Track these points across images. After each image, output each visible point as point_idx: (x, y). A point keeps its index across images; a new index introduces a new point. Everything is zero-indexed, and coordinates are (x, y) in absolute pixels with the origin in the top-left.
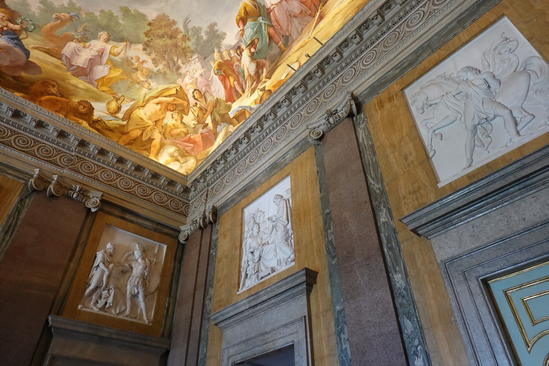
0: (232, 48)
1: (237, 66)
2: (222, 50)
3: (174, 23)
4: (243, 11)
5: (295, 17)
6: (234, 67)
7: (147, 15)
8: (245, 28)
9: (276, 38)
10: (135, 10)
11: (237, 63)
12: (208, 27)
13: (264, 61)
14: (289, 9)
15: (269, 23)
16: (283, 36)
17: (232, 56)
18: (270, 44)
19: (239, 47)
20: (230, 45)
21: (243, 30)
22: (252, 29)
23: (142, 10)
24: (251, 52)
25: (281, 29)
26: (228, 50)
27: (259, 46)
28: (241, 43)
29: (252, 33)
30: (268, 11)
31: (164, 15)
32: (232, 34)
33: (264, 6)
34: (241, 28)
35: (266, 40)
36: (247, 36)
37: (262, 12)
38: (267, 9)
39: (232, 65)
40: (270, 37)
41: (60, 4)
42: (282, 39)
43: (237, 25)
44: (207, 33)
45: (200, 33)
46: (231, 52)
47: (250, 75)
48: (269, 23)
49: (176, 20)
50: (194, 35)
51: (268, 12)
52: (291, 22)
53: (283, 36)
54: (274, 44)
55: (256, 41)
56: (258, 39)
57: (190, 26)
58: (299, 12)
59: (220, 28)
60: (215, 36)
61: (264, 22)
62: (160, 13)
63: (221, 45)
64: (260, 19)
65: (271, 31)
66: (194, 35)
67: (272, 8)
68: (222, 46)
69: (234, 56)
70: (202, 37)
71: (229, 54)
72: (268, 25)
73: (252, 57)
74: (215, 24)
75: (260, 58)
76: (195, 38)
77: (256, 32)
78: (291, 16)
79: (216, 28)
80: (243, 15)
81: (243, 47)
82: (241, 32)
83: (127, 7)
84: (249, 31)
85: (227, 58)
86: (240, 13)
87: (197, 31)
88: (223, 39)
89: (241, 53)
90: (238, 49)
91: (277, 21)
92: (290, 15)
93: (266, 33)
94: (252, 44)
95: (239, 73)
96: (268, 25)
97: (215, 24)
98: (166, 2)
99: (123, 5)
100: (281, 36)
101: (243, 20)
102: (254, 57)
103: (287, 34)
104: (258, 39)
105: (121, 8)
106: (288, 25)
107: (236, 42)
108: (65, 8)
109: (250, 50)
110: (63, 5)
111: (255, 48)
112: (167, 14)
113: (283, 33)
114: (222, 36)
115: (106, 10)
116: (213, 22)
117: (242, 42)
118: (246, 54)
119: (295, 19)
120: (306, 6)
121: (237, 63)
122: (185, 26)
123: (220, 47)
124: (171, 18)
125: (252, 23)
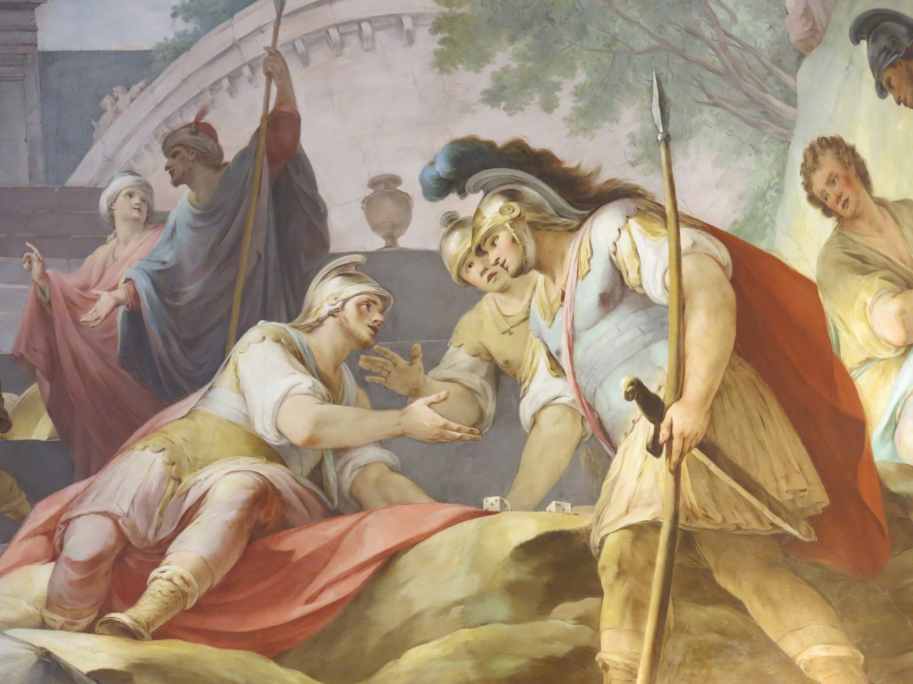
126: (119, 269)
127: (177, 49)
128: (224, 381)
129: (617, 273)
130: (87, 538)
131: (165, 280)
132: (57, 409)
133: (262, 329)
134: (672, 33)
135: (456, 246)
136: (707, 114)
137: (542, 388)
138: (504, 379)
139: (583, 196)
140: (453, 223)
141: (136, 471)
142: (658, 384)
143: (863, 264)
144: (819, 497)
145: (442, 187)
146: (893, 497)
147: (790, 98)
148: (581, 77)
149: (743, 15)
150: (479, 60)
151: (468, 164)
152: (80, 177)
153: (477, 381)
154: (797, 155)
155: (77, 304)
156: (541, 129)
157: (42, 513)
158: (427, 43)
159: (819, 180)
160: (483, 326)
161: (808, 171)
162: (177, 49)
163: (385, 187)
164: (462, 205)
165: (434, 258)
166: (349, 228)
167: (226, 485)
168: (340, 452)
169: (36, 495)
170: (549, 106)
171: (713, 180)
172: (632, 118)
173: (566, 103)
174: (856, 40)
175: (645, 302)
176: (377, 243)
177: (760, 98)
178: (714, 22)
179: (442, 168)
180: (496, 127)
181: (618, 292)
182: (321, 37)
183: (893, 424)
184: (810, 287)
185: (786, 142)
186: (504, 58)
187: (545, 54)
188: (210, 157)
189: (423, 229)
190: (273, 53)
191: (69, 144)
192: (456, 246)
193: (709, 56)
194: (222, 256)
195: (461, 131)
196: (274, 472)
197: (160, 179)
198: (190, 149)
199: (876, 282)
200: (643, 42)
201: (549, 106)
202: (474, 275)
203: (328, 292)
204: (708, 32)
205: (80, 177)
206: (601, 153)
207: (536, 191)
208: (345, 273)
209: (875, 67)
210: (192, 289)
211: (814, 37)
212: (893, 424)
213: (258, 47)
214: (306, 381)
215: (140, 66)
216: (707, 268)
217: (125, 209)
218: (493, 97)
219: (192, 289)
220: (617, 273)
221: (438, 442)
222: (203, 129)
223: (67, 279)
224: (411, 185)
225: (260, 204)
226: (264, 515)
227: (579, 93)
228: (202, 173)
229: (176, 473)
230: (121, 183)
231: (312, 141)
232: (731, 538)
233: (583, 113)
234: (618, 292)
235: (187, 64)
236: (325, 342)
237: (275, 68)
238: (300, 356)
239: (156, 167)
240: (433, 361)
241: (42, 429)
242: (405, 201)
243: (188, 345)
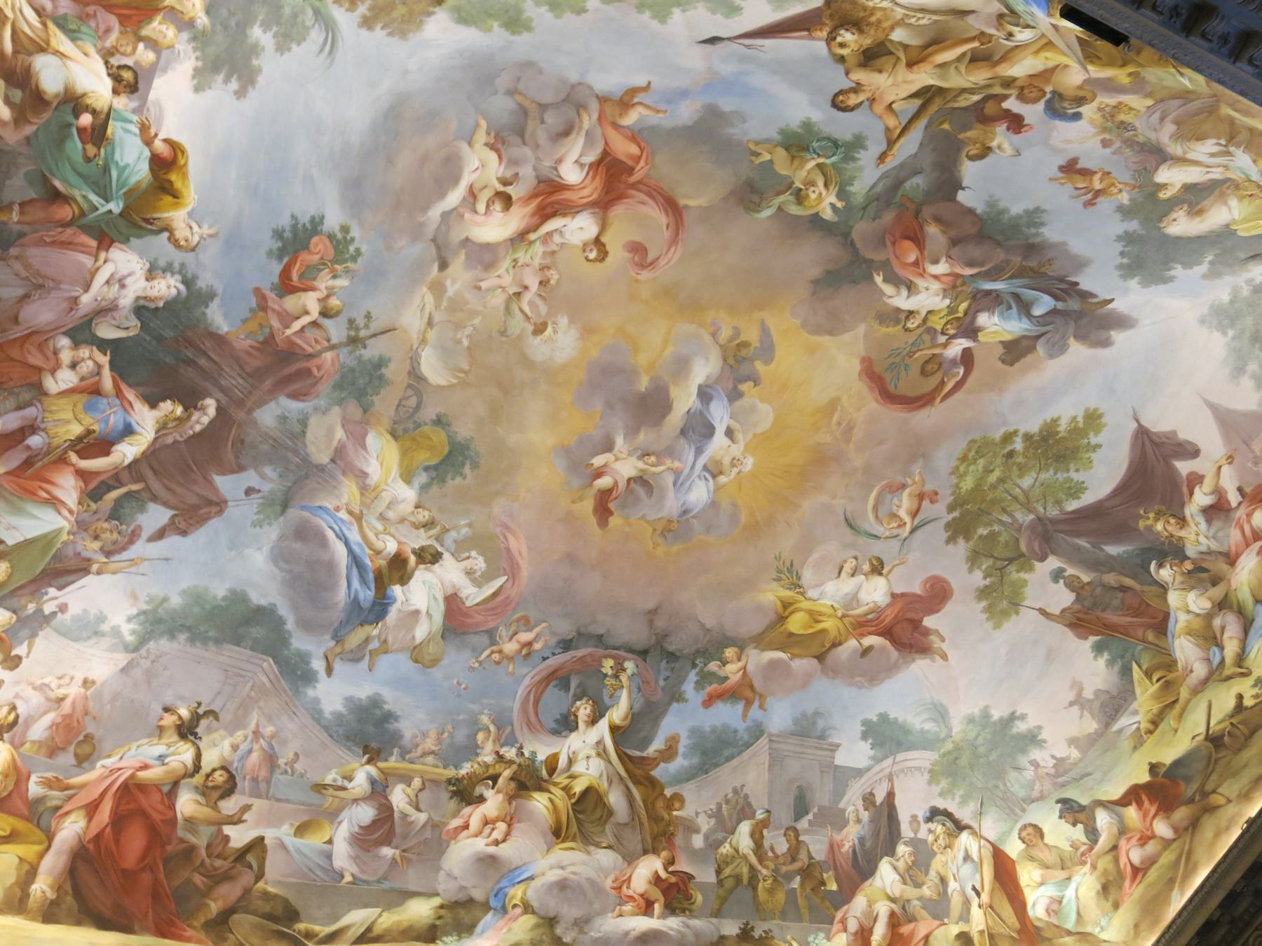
0: (152, 70)
1: (108, 31)
2: (185, 36)
3: (367, 23)
4: (178, 184)
5: (25, 297)
6: (113, 21)
7: (452, 25)
8: (147, 153)
9: (38, 213)
10: (490, 30)
11: (111, 41)
12: (259, 70)
13: (29, 130)
14: (54, 294)
15: (84, 221)
16: (21, 235)
17: (141, 46)
18: (45, 181)
19: (132, 88)
20: (165, 70)
21: (148, 143)
22: (127, 166)
23: (470, 37)
24: (87, 109)
25: (41, 243)
26: (165, 54)
27: (75, 146)
28: (134, 104)
29: (117, 157)
30: (107, 240)
31: (403, 35)
32: (180, 102)
33: (126, 240)
34: (159, 145)
35: (65, 181)
36: (127, 137)
37: (122, 225)
38: (112, 242)
39: (123, 20)
40: (56, 197)
41: (691, 13)
42: (19, 227)
43: (175, 137)
44: (255, 49)
45: (275, 36)
46: (150, 56)
47: (42, 48)
48: (84, 221)
49: (364, 32)
50: (295, 16)
51: (105, 236)
52: (26, 279)
53: (21, 235)
54: (32, 194)
55: (91, 150)
56: (88, 160)
57: (316, 35)
58: (23, 315)
59: (221, 91)
60: (228, 61)
61: (102, 210)
62: (414, 38)
63: (195, 49)
64: (116, 207)
65: (66, 212)
66: (295, 16)
67: (103, 255)
68: (190, 47)
69: (135, 49)
70: (266, 26)
71: (153, 44)
72: (83, 214)
73: (73, 102)
74: (240, 94)
75: (46, 125)
76: (287, 11)
77: (106, 169)
78: (38, 285)
79: (234, 85)
80: (173, 177)
81: (123, 103)
82: (153, 132)
83: (513, 33)
84: (131, 158)
85: (158, 28)
86: (184, 176)
87: (288, 37)
88: (197, 72)
89: (116, 79)
90: (129, 82)
91: (68, 245)
92: (41, 286)
93: (77, 194)
94: (98, 134)
95: (84, 18)
96: (83, 214)
97: (240, 94)
98: (406, 72)
99: (526, 37)
100: (26, 228)
101: (166, 165)
102: (68, 108)
103: (13, 251)
104: (88, 160)
105: (529, 28)
106: (27, 266)
107: (152, 96)
108: (679, 5)
109: (94, 112)
110: (684, 11)
111: (81, 131)
112: (395, 41)
113: (26, 240)
114: (201, 79)
115: (569, 16)
116: (252, 94)
117: (134, 111)
118: (94, 82)
119: (20, 292)
120: (15, 340)
121: (111, 41)
122: (330, 27)
123: (194, 39)
124: (379, 33)
125: (133, 180)
126: (850, 836)
127: (868, 769)
128: (878, 874)
129: (966, 851)
130: (853, 926)
131: (862, 840)
132: (838, 880)
133: (886, 860)
134: (990, 785)
135: (931, 838)
136: (994, 808)
137: (953, 885)
138: (943, 880)
139: (960, 827)
140: (930, 831)
141: (859, 903)
142: (978, 887)
143: (1032, 859)
144: (1017, 925)
145: (929, 820)
146: (1036, 927)
147: (1024, 811)
148: (962, 792)
149: (1016, 787)
150: (938, 783)
151: (934, 814)
152: (841, 805)
153: (937, 881)
154: (1019, 825)
155: (840, 846)
156: (952, 807)
157: (839, 915)
158: (927, 776)
159: (1024, 834)
160: (937, 864)
161: (1021, 831)
162: (868, 769)
163: (914, 817)
164: (932, 826)
165: (925, 841)
166: (906, 830)
167: (883, 909)
168: (908, 901)
169: (837, 908)
170: (953, 799)
171: (991, 827)
172: (973, 806)
173: (957, 799)
174: (1058, 802)
175: (973, 861)
176: (912, 835)
177: (1012, 806)
178: (1005, 785)
179: (928, 814)
180: (941, 804)
181: (967, 857)
182: (902, 770)
183: (1034, 905)
184: (1013, 862)
185: (1016, 821)
186: (944, 783)
187: (954, 784)
188: (873, 803)
189: (922, 834)
190: (891, 774)
191: (839, 794)
192: (931, 838)
193: (1000, 795)
194: (876, 834)
195: (933, 804)
196: (893, 905)
197: (861, 808)
198: (868, 799)
199: (1035, 864)
200: (980, 786)
201: (953, 799)
202: (935, 848)
203: (902, 849)
204: (1002, 787)
205: (841, 805)
206: (964, 814)
207: (949, 824)
208: (905, 844)
209: (1061, 811)
210: (868, 844)
211: (1041, 798)
212: (1034, 905)
213: (887, 772)
214: (898, 877)
215: (859, 773)
216: (987, 852)
217: (852, 817)
218: (941, 794)
219: (868, 844)
220: (966, 851)
221: (930, 900)
222: (872, 794)
223: (837, 837)
224: (921, 819)
225: (885, 819)
226: (894, 922)
227: (961, 796)
228: (871, 808)
229: (870, 904)
230: (851, 808)
231: (898, 802)
232: (1001, 935)
233: (961, 803)
234: (967, 857)
235: (869, 774)
236: (901, 865)
237: (891, 779)
238: (895, 868)
239: (860, 803)
240: (927, 874)
241: (833, 887)
242: (918, 823)
243: (868, 862)
